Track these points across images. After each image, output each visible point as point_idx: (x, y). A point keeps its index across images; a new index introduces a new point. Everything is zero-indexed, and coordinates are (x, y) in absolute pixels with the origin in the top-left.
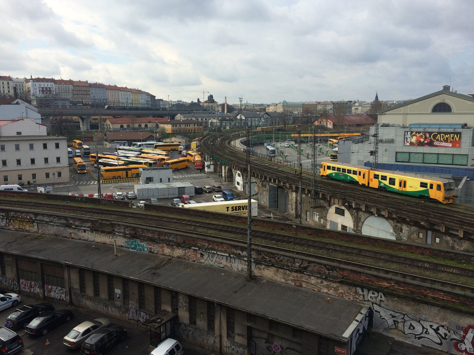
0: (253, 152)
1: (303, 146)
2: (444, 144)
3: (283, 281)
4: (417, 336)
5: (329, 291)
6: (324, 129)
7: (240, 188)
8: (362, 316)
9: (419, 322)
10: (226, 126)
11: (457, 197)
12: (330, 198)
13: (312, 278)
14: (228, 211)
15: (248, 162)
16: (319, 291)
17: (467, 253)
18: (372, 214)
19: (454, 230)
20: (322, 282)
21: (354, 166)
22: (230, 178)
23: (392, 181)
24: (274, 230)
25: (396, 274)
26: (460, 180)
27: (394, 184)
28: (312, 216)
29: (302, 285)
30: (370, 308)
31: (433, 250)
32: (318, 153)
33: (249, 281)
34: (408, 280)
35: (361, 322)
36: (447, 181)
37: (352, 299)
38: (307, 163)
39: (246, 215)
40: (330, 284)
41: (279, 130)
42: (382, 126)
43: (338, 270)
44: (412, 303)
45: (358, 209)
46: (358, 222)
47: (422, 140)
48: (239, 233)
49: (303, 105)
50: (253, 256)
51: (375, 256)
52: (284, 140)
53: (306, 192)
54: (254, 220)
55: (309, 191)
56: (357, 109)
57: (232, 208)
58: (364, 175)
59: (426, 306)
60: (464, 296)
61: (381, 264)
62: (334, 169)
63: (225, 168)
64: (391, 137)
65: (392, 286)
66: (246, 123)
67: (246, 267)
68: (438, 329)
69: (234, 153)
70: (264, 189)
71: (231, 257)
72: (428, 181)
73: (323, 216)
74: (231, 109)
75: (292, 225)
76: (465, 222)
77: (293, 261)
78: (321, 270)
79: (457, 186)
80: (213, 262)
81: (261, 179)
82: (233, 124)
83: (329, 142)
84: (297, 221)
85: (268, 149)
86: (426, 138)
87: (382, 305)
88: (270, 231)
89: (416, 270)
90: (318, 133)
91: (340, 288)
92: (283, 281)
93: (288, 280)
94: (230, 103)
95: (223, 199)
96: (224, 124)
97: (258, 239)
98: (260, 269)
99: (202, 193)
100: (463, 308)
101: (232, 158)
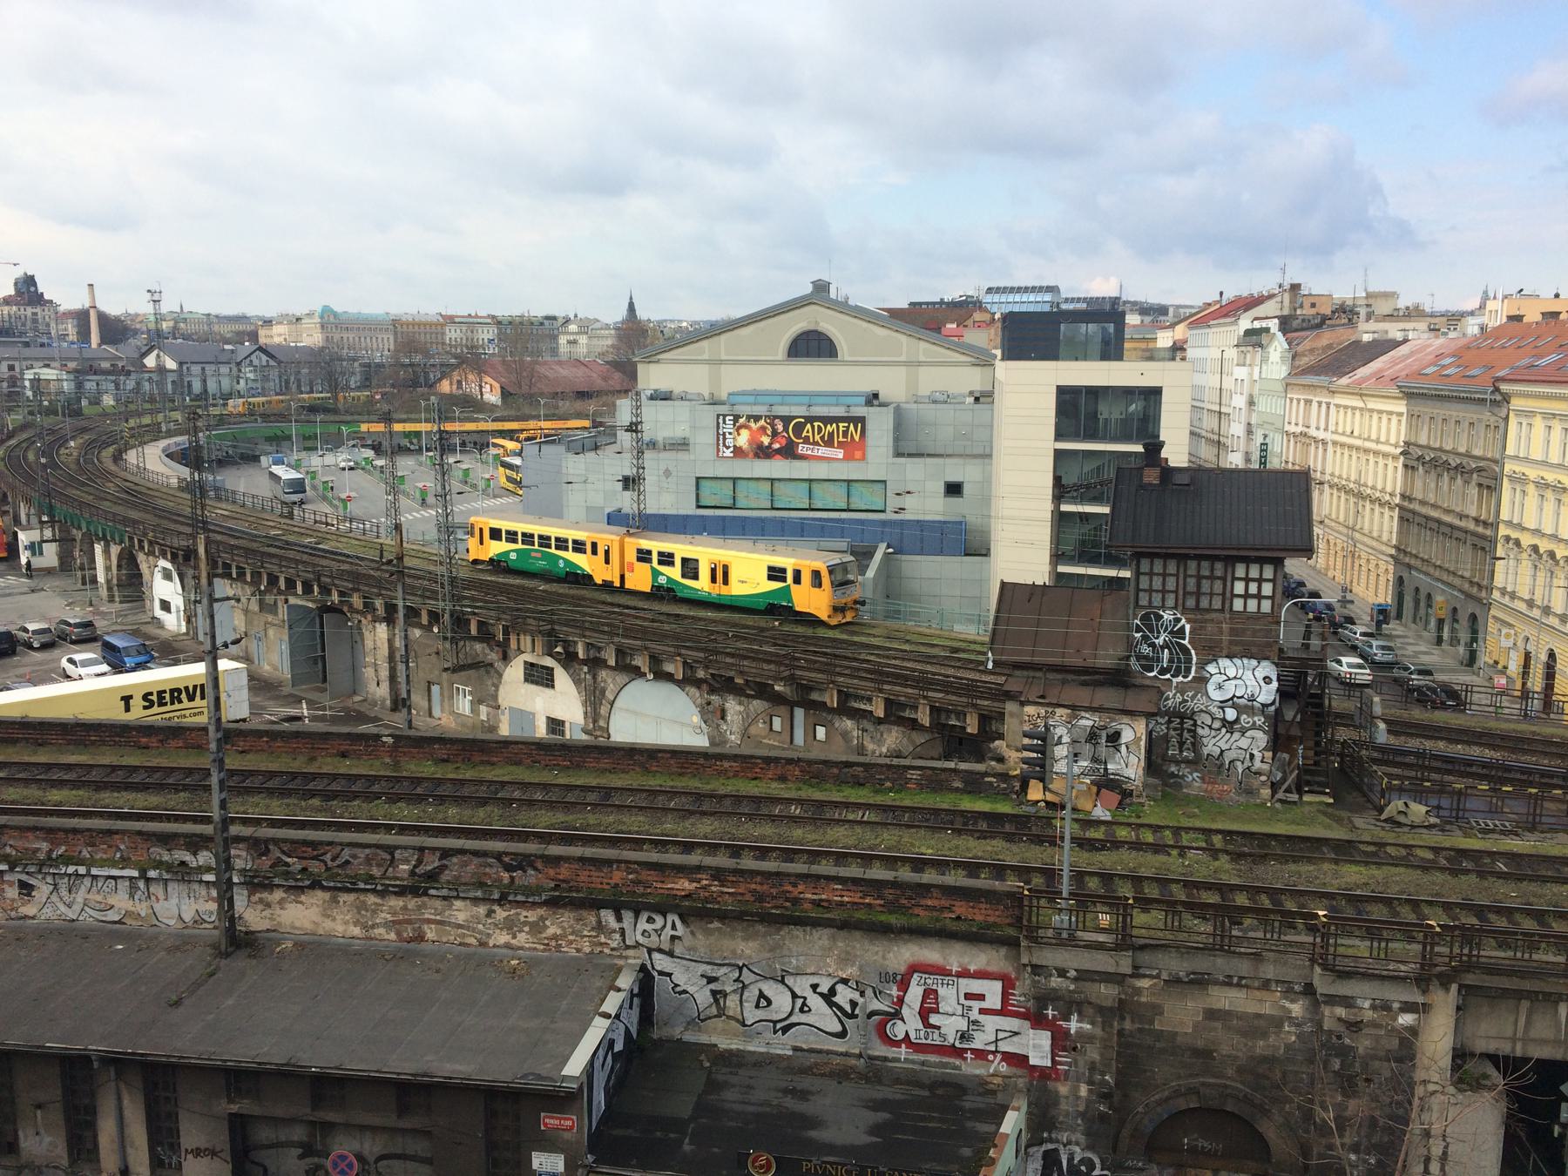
0: (217, 489)
1: (405, 464)
2: (822, 451)
3: (357, 931)
4: (779, 1026)
5: (514, 937)
6: (473, 406)
7: (173, 622)
8: (622, 995)
9: (782, 982)
10: (99, 393)
11: (863, 603)
12: (506, 632)
13: (458, 904)
14: (127, 709)
15: (201, 524)
16: (483, 944)
17: (895, 761)
18: (637, 673)
19: (861, 698)
20: (490, 913)
21: (576, 525)
22: (132, 585)
23: (690, 567)
24: (312, 759)
25: (713, 848)
26: (869, 554)
27: (696, 577)
28: (449, 696)
29: (425, 933)
30: (643, 968)
31: (810, 762)
32: (456, 486)
33: (227, 955)
34: (748, 863)
35: (617, 1016)
36: (835, 559)
37: (587, 950)
38: (420, 522)
39: (203, 719)
40: (518, 914)
41: (313, 409)
42: (652, 398)
43: (539, 865)
44: (761, 928)
45: (596, 663)
46: (595, 701)
47: (766, 440)
48: (177, 788)
49: (396, 323)
50: (239, 864)
51: (652, 804)
52: (335, 443)
53: (425, 620)
54: (232, 735)
55: (435, 617)
56: (575, 342)
57: (146, 697)
58: (607, 553)
59: (798, 932)
60: (894, 884)
61: (670, 827)
62: (512, 536)
63: (107, 552)
64: (680, 431)
65: (704, 888)
66: (181, 384)
67: (213, 906)
68: (832, 991)
69: (139, 495)
70: (270, 618)
71: (148, 880)
72: (788, 562)
73: (486, 697)
74: (114, 329)
75: (378, 737)
76: (888, 674)
77: (389, 857)
78: (485, 874)
79: (863, 570)
80: (77, 907)
81: (256, 582)
82: (131, 384)
83: (493, 451)
84: (399, 719)
85: (274, 477)
86: (775, 434)
87: (677, 952)
88: (298, 764)
89: (768, 830)
90: (453, 420)
91: (548, 923)
92: (357, 931)
93: (373, 927)
94: (113, 307)
95: (105, 668)
96: (90, 386)
97: (256, 799)
98: (268, 905)
99: (14, 653)
100: (893, 919)
101: (134, 514)
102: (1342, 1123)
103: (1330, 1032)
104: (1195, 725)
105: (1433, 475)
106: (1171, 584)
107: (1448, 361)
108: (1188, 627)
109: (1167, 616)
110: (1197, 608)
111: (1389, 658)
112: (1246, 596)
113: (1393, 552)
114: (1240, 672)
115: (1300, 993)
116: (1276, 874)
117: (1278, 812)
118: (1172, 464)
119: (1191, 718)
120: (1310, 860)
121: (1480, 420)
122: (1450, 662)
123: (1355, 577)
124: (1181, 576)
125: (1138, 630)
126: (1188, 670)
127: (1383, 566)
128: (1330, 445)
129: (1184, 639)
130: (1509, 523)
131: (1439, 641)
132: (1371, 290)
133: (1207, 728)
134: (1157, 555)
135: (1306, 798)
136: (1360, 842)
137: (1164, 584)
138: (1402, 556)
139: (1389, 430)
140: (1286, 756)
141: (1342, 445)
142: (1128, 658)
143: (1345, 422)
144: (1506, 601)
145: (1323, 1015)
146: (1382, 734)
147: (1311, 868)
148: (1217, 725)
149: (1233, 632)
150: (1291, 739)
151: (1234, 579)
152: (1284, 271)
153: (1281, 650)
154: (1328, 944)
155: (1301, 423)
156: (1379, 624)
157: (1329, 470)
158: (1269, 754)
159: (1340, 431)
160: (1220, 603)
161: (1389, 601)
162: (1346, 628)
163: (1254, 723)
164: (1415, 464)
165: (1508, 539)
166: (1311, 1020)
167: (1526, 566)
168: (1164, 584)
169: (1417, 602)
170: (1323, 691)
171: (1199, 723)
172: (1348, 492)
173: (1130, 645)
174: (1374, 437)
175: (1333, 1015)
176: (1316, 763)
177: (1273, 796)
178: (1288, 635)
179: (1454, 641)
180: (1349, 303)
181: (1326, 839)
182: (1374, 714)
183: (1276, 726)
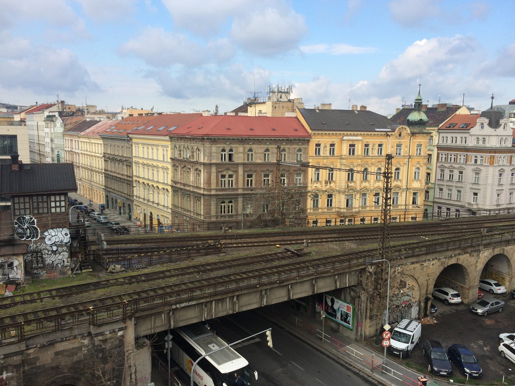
102: (104, 374)
103: (98, 345)
104: (42, 254)
105: (113, 163)
106: (27, 206)
107: (113, 128)
108: (35, 221)
109: (27, 217)
110: (38, 213)
111: (106, 221)
112: (56, 207)
113: (104, 187)
114: (56, 233)
115: (87, 336)
116: (75, 299)
117: (74, 278)
118: (23, 162)
119: (40, 252)
120: (86, 291)
121: (124, 146)
122: (124, 219)
123: (93, 196)
124: (31, 203)
125: (16, 224)
126: (37, 236)
127: (101, 192)
128: (80, 154)
129: (35, 225)
130: (136, 176)
131: (120, 213)
132: (88, 104)
133: (46, 255)
134: (21, 196)
135: (83, 271)
136: (102, 281)
137: (25, 206)
138: (107, 189)
139: (98, 149)
140: (75, 259)
141: (84, 154)
142: (13, 235)
143: (84, 147)
144: (138, 199)
145: (95, 340)
146: (105, 246)
147: (87, 294)
148: (50, 253)
149: (52, 220)
150: (76, 253)
151: (51, 201)
152: (58, 96)
153: (70, 224)
154: (94, 317)
155: (70, 147)
156: (102, 210)
157: (81, 162)
158: (69, 259)
159: (83, 150)
160: (47, 210)
161: (104, 203)
162: (92, 213)
163: (63, 249)
164: (107, 159)
165: (136, 181)
166: (91, 344)
167: (142, 188)
168: (25, 206)
169: (113, 202)
170: (85, 234)
171: (43, 253)
172: (88, 169)
173: (14, 230)
174: (94, 151)
175: (97, 340)
176: (86, 259)
177: (72, 273)
178: (72, 218)
179: (125, 213)
180: (81, 108)
181: (91, 283)
182: (102, 240)
183: (71, 250)
